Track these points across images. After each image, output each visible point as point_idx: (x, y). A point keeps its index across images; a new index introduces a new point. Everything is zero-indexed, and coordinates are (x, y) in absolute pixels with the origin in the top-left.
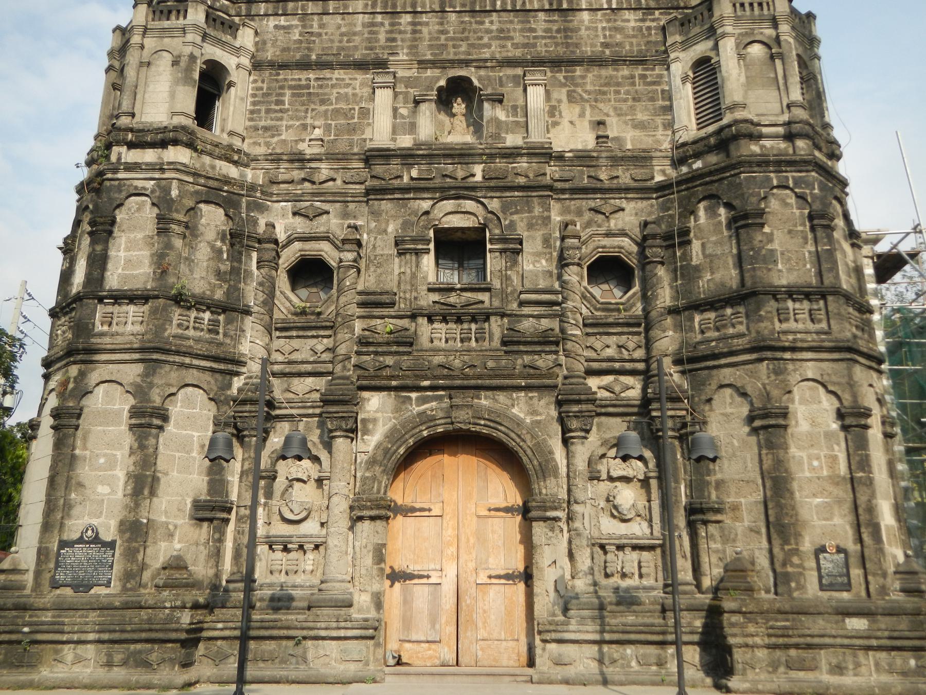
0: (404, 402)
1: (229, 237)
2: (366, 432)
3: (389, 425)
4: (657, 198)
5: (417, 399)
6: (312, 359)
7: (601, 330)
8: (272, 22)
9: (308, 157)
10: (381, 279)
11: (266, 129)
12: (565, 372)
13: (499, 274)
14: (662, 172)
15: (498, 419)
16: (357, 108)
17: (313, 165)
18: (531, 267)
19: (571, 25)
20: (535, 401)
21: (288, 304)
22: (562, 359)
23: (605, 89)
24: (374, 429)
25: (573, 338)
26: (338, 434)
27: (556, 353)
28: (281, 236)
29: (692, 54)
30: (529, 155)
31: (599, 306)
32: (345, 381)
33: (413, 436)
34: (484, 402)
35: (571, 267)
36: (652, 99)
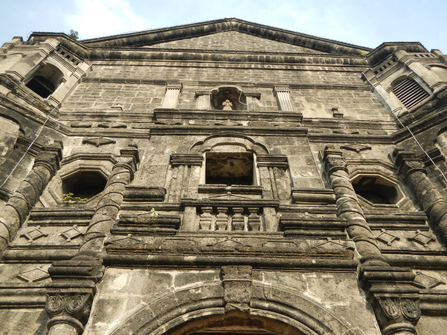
0: (160, 281)
1: (15, 143)
2: (100, 317)
3: (136, 308)
4: (395, 144)
5: (178, 278)
6: (59, 244)
7: (385, 225)
8: (103, 67)
9: (107, 114)
10: (153, 181)
11: (80, 104)
12: (360, 256)
13: (269, 181)
14: (390, 131)
15: (288, 301)
16: (152, 99)
17: (109, 119)
18: (299, 176)
19: (301, 75)
20: (332, 283)
21: (52, 200)
22: (352, 244)
23: (332, 98)
24: (113, 313)
25: (360, 223)
26: (60, 317)
27: (343, 237)
28: (67, 152)
29: (389, 80)
30: (284, 117)
31: (373, 208)
32: (91, 257)
33: (167, 321)
34: (264, 282)
35: (339, 171)
36: (368, 102)
